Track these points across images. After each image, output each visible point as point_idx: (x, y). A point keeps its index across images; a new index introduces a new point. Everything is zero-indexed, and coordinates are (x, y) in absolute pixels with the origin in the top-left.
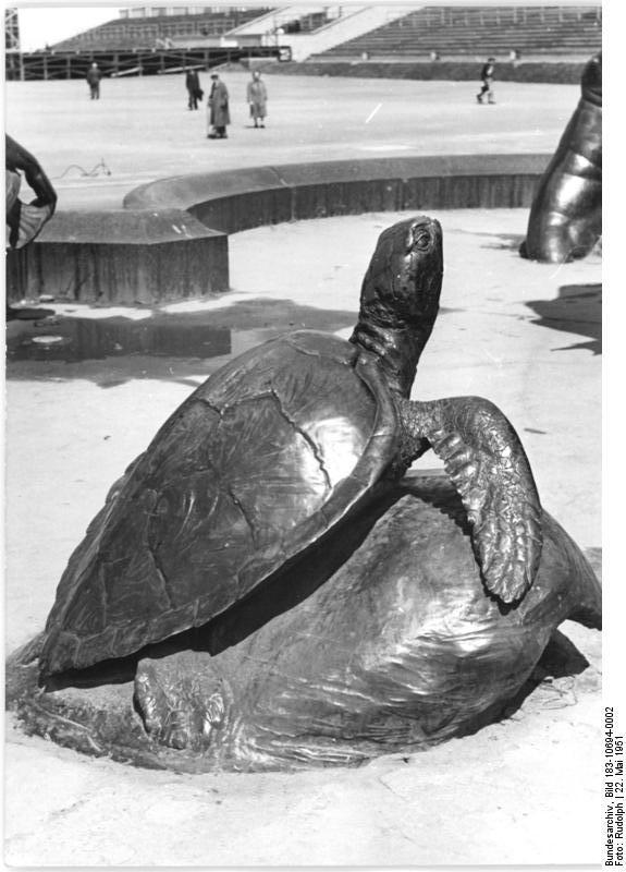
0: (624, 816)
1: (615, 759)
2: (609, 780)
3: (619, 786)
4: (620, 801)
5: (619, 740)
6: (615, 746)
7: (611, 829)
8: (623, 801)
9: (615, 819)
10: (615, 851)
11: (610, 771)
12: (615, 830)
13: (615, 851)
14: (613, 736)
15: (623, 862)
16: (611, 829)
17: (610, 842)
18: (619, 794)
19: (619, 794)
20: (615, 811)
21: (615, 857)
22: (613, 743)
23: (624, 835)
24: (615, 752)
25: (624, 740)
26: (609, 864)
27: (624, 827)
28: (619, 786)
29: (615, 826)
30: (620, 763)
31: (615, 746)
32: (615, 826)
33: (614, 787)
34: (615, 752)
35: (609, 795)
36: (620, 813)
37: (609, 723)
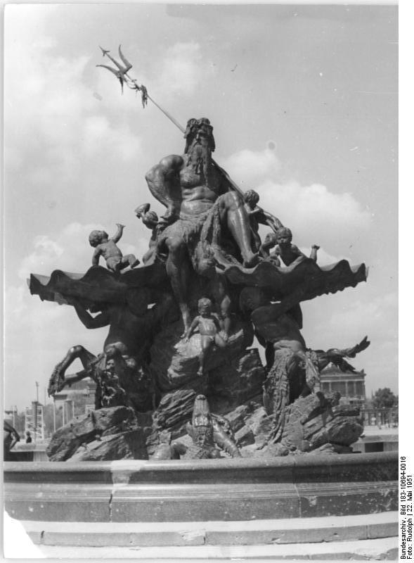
0: (413, 527)
1: (407, 490)
2: (403, 503)
3: (409, 508)
4: (410, 517)
5: (410, 477)
6: (407, 481)
7: (404, 536)
8: (413, 517)
9: (407, 529)
10: (407, 549)
11: (404, 498)
12: (407, 536)
13: (407, 549)
14: (405, 475)
15: (412, 557)
16: (404, 536)
17: (404, 543)
18: (410, 512)
19: (410, 512)
20: (407, 524)
21: (407, 553)
22: (406, 480)
23: (413, 539)
24: (407, 485)
25: (413, 478)
26: (403, 557)
27: (413, 534)
28: (409, 508)
29: (407, 534)
30: (410, 493)
31: (406, 483)
32: (407, 534)
33: (406, 508)
34: (407, 485)
35: (403, 513)
36: (410, 525)
37: (403, 467)
